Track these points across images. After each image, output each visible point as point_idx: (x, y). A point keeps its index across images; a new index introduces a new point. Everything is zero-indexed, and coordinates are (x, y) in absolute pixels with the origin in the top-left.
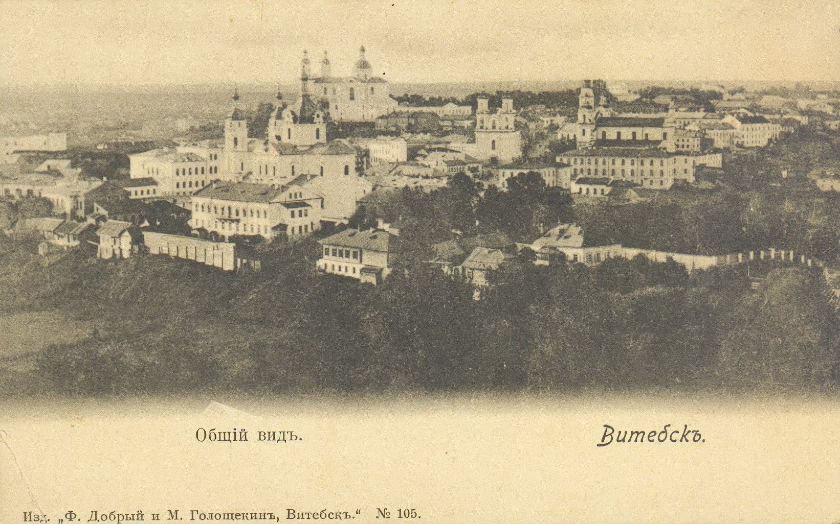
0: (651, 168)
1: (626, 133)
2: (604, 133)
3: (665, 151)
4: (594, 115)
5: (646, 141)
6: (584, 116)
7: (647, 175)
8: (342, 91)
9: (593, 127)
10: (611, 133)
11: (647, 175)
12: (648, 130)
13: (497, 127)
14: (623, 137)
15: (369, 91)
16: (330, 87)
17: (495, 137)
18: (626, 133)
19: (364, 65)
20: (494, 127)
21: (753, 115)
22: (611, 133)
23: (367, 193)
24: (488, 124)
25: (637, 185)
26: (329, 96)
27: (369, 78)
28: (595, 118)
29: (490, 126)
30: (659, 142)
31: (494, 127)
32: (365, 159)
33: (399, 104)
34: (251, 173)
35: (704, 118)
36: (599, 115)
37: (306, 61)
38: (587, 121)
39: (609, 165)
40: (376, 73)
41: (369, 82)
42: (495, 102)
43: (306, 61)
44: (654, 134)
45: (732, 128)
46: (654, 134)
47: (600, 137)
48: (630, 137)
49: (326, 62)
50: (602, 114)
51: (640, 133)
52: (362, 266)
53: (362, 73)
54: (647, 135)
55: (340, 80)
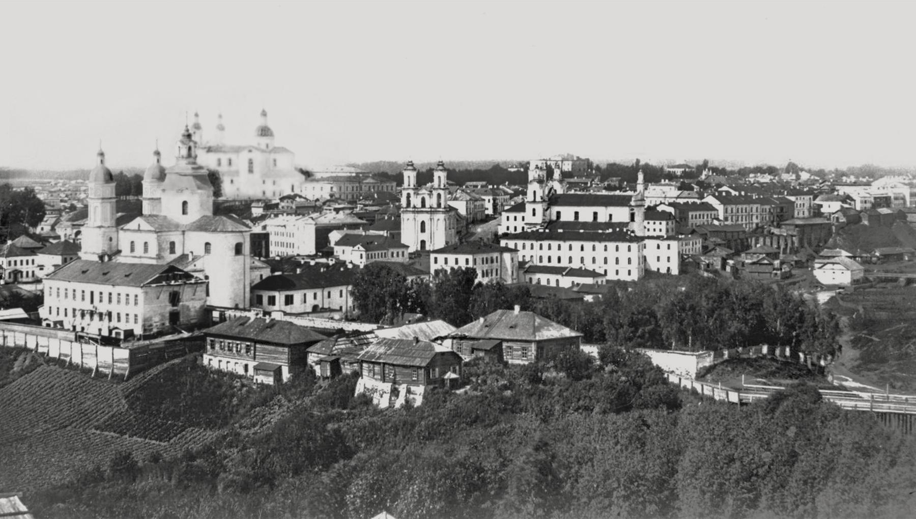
0: (605, 254)
1: (586, 214)
2: (558, 213)
3: (632, 235)
4: (547, 192)
5: (609, 224)
6: (535, 192)
7: (611, 261)
8: (241, 162)
9: (545, 205)
10: (567, 214)
11: (611, 261)
12: (612, 210)
13: (427, 205)
14: (582, 219)
15: (272, 162)
16: (224, 158)
17: (425, 217)
18: (586, 214)
19: (265, 132)
20: (423, 205)
21: (737, 193)
22: (567, 214)
23: (264, 277)
24: (416, 201)
25: (599, 275)
26: (223, 169)
27: (270, 148)
28: (548, 195)
29: (419, 205)
30: (626, 224)
31: (423, 205)
32: (263, 243)
33: (306, 179)
34: (119, 252)
35: (678, 197)
36: (553, 191)
37: (187, 126)
38: (538, 199)
39: (588, 254)
40: (277, 141)
41: (270, 152)
42: (424, 178)
43: (187, 126)
44: (620, 214)
45: (714, 209)
46: (620, 214)
47: (554, 218)
48: (590, 219)
49: (221, 128)
50: (555, 191)
51: (603, 214)
52: (255, 363)
53: (264, 141)
54: (611, 216)
55: (237, 150)
